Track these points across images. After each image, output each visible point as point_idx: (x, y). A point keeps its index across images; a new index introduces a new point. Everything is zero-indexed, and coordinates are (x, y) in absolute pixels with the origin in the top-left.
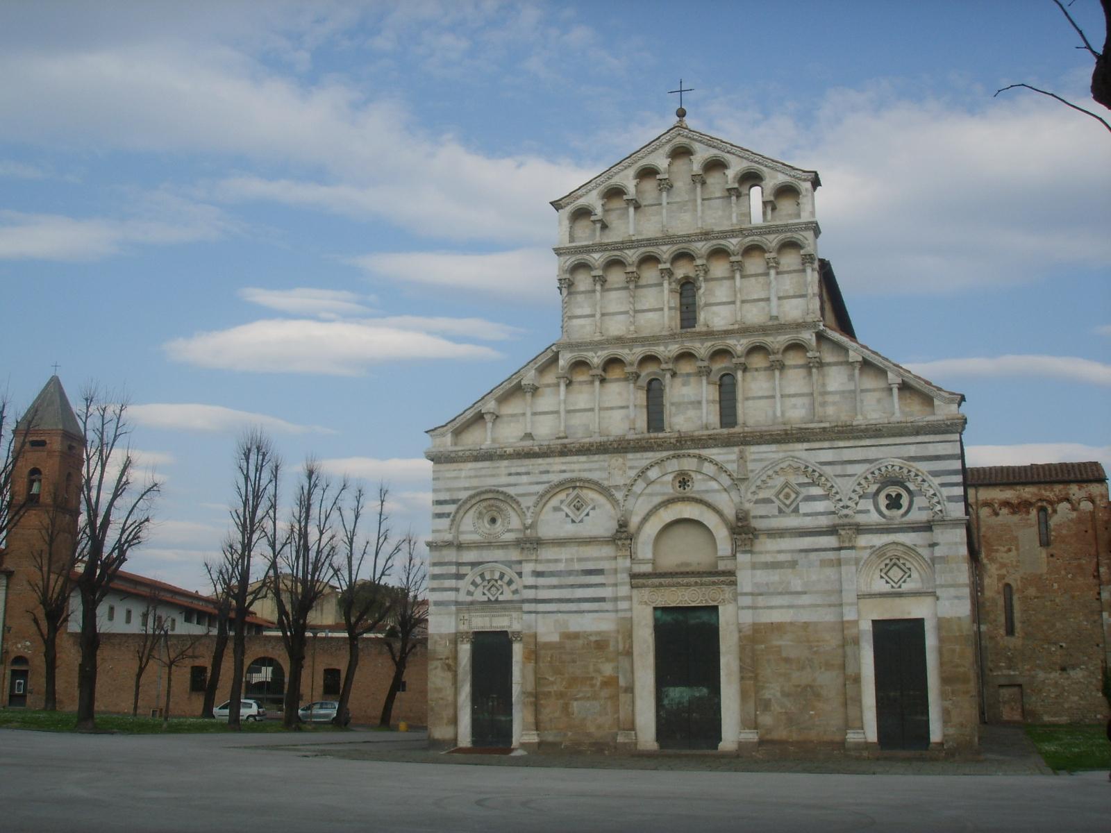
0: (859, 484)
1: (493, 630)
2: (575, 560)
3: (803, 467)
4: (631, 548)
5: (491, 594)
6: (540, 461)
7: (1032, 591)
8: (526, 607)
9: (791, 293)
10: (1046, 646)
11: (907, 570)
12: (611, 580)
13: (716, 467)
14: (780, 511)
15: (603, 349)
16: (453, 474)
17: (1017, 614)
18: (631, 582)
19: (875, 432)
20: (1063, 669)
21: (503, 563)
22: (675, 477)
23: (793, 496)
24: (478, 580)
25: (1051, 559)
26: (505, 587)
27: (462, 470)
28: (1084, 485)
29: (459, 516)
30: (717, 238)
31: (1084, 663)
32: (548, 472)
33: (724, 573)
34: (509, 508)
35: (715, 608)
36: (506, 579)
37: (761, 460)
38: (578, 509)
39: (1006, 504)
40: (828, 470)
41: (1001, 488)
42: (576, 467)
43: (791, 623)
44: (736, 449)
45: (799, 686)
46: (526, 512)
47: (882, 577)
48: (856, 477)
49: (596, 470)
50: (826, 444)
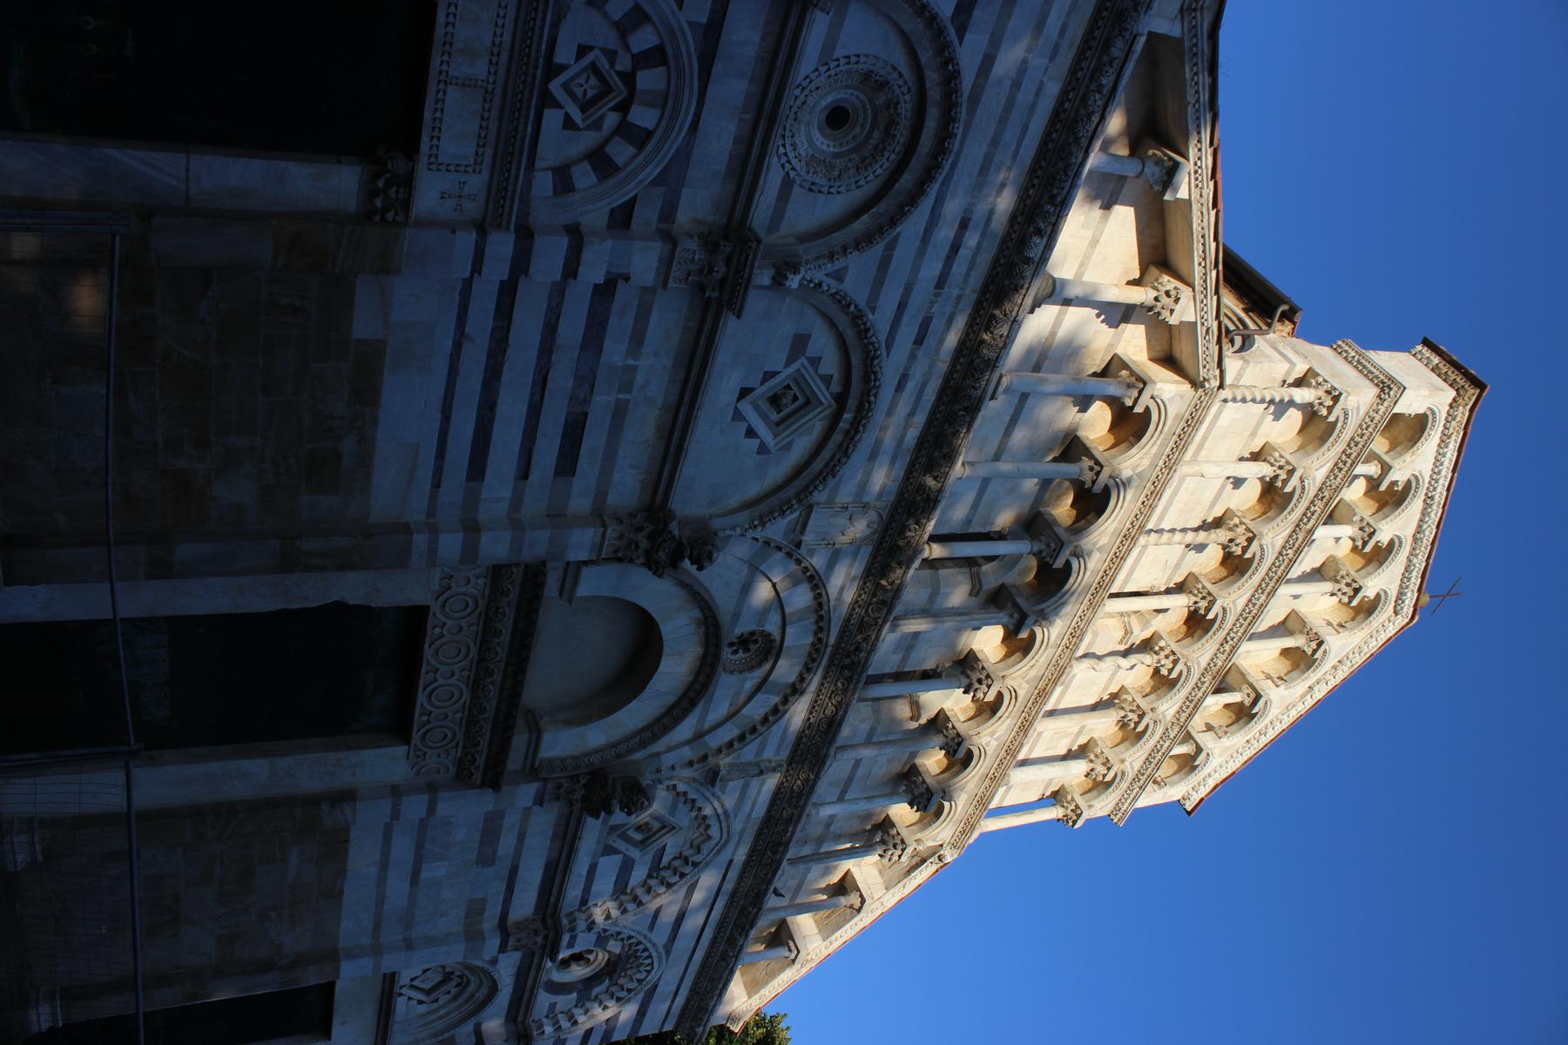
1: (432, 86)
2: (620, 396)
3: (697, 859)
5: (573, 78)
8: (502, 246)
11: (433, 996)
12: (534, 504)
13: (758, 718)
18: (517, 565)
21: (684, 155)
24: (643, 39)
26: (588, 140)
27: (1052, 58)
32: (919, 341)
34: (858, 195)
35: (398, 727)
36: (621, 152)
38: (775, 401)
43: (342, 873)
46: (830, 267)
47: (425, 971)
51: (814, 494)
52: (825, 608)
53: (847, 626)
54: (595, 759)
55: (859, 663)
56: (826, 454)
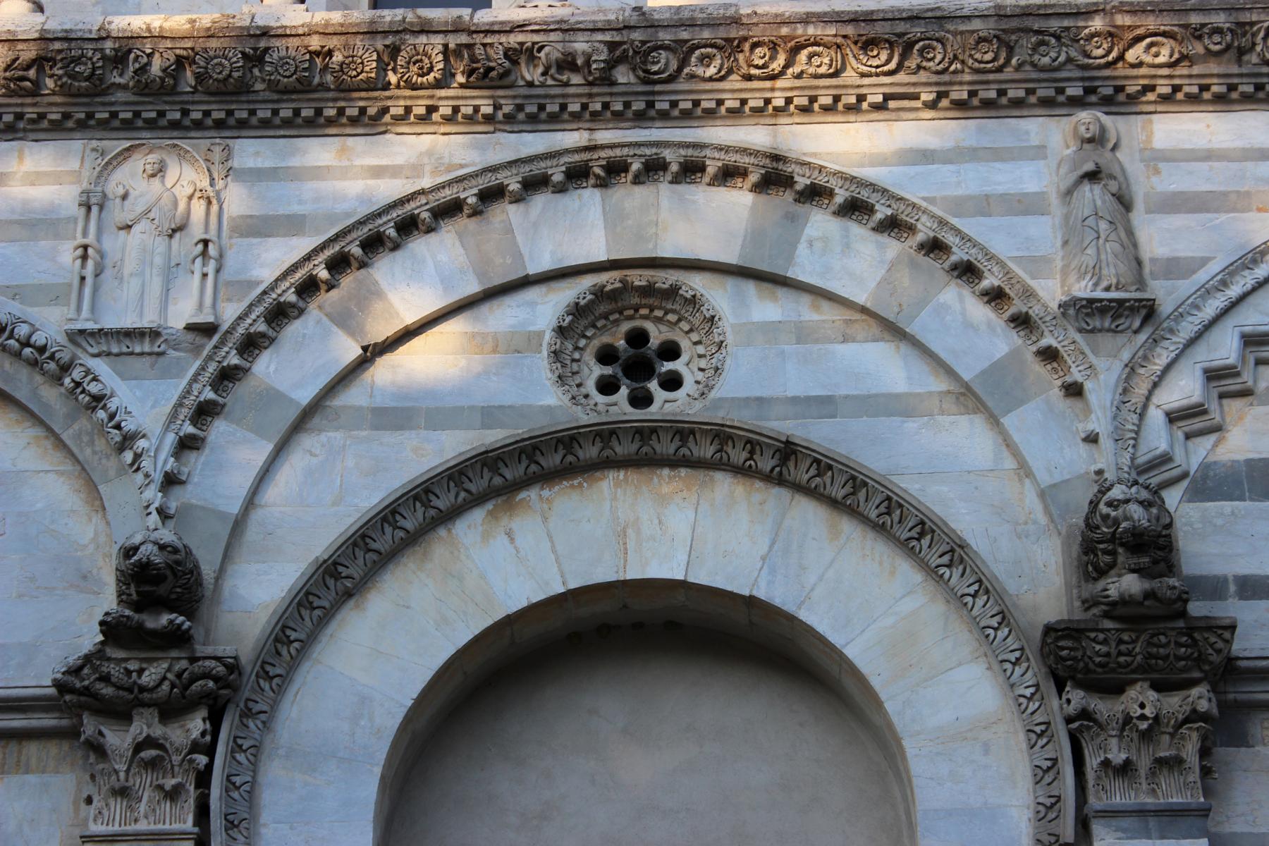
4: (203, 779)
13: (893, 247)
22: (577, 311)
51: (41, 342)
52: (448, 194)
53: (509, 118)
54: (1030, 675)
55: (612, 46)
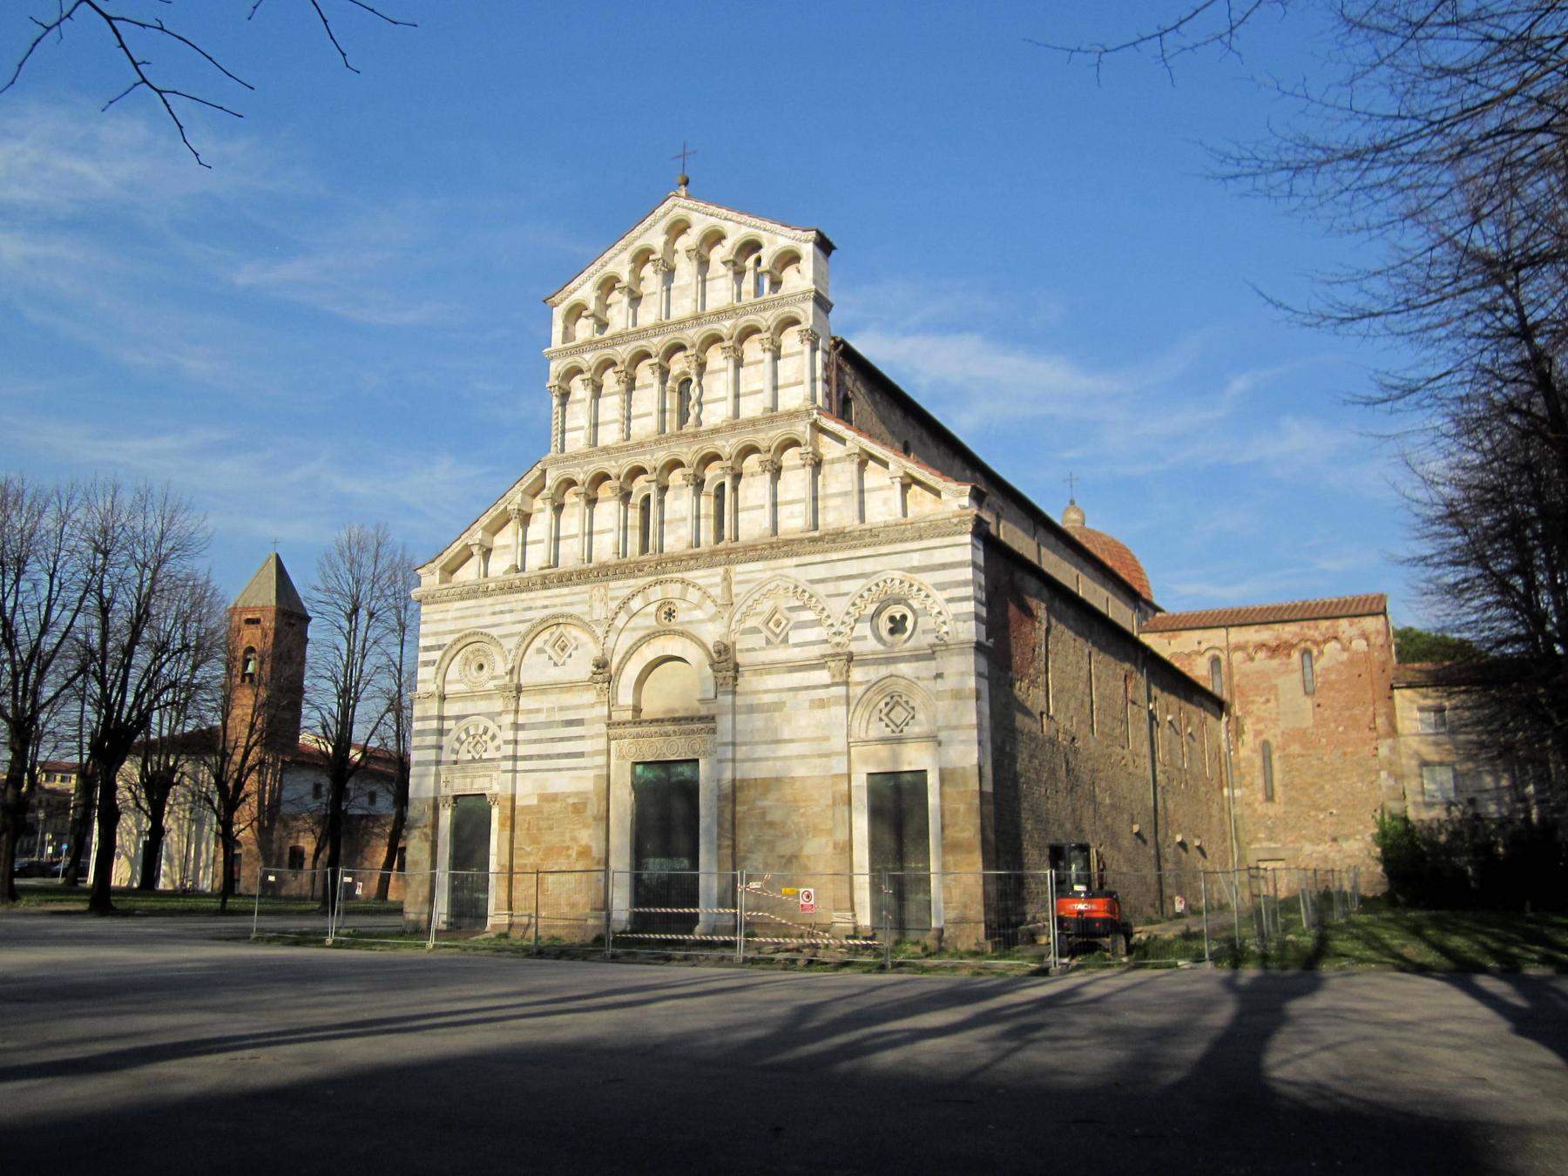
0: (854, 604)
6: (523, 596)
7: (1295, 748)
9: (792, 380)
10: (1313, 813)
14: (768, 641)
15: (589, 463)
16: (441, 616)
17: (1278, 776)
19: (871, 537)
20: (1334, 840)
23: (784, 622)
24: (463, 736)
25: (1317, 709)
26: (489, 742)
28: (1356, 620)
29: (444, 665)
30: (710, 322)
31: (1358, 832)
32: (530, 608)
33: (701, 719)
36: (490, 733)
37: (748, 581)
39: (1261, 646)
40: (821, 589)
41: (1257, 627)
42: (557, 601)
44: (721, 570)
45: (783, 857)
47: (881, 719)
48: (846, 598)
49: (579, 603)
50: (818, 558)
56: (575, 622)
